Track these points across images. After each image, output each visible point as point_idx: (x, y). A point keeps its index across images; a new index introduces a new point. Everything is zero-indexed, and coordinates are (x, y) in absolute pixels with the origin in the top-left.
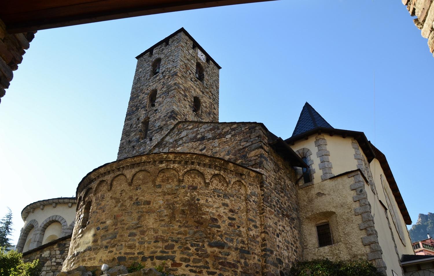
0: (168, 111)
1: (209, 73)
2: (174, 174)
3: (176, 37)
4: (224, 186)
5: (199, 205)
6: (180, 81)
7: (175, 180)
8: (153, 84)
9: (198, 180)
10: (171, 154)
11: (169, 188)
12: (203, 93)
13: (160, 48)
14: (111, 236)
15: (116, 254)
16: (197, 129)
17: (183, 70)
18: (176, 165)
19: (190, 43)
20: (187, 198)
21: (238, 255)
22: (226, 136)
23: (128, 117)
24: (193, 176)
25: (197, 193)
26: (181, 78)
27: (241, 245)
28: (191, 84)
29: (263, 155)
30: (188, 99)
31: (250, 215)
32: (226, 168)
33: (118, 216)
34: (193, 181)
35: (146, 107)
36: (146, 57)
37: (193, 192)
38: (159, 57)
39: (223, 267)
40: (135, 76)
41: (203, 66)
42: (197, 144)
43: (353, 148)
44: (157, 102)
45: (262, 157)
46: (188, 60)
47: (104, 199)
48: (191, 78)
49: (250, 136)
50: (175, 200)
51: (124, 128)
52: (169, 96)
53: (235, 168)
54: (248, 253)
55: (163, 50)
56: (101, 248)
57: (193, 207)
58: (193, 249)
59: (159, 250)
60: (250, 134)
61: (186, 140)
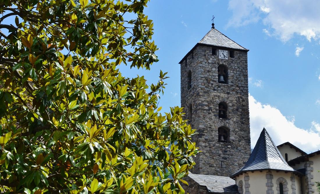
12: (228, 93)
17: (204, 87)
19: (209, 52)
43: (266, 178)
46: (209, 71)
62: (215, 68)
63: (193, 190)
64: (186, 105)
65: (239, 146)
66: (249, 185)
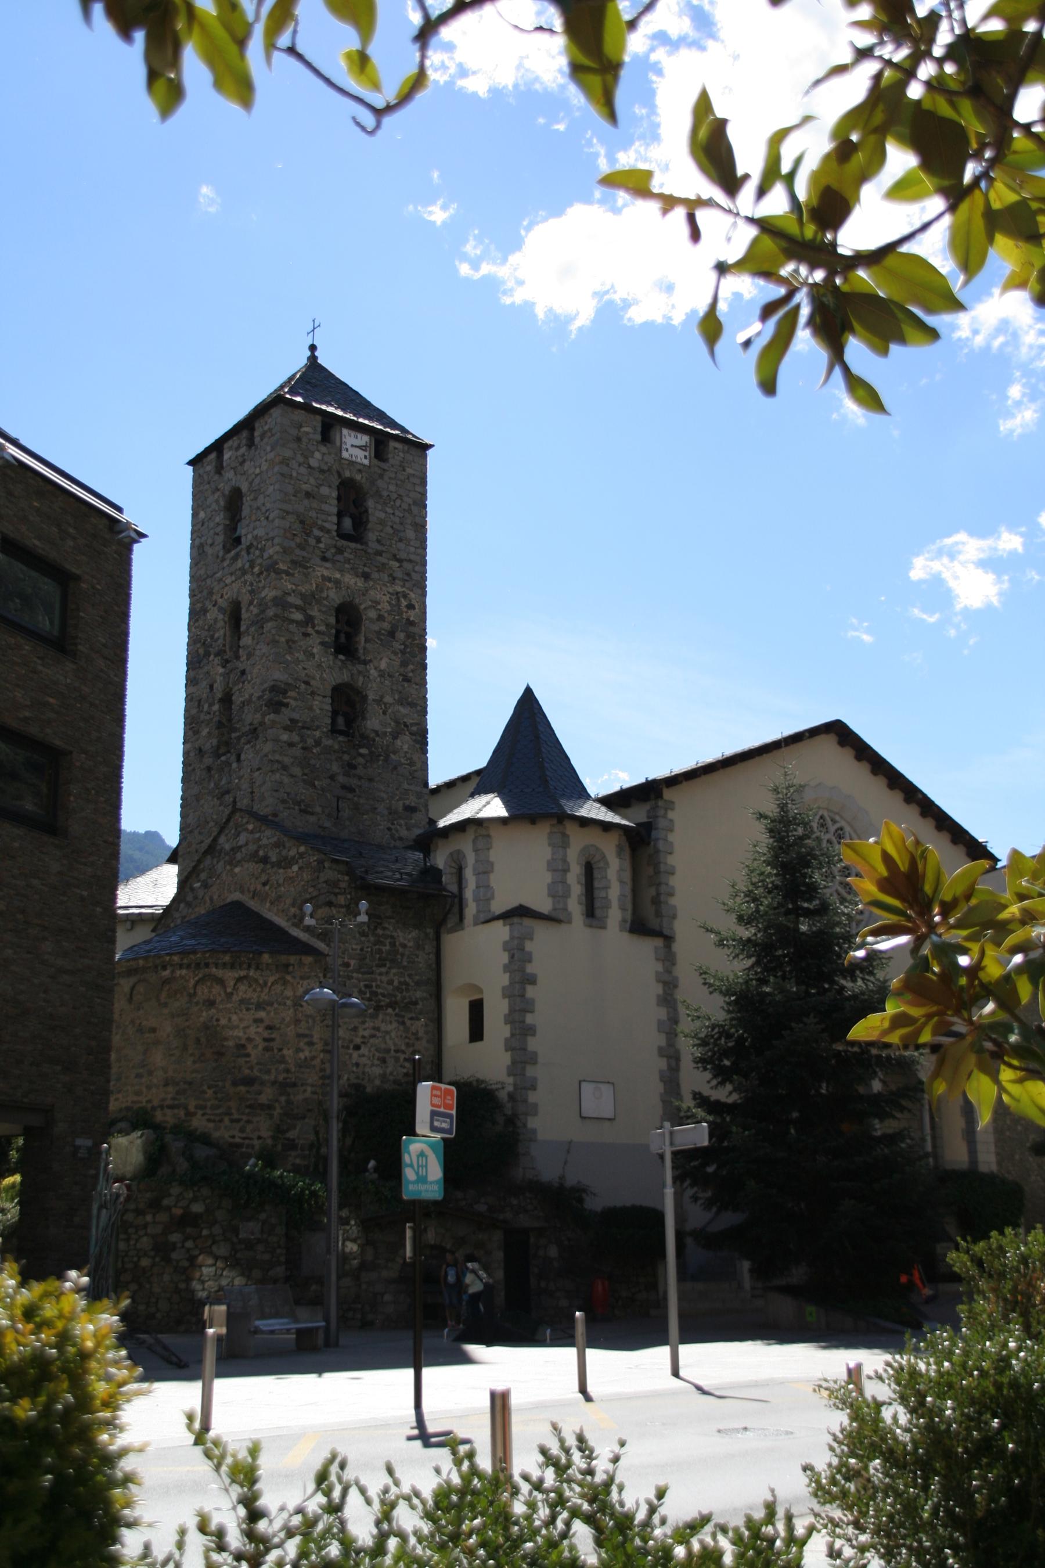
1: (385, 494)
9: (217, 989)
12: (366, 576)
18: (184, 972)
24: (209, 984)
26: (288, 574)
30: (317, 628)
35: (225, 651)
41: (364, 480)
43: (550, 845)
46: (308, 495)
50: (187, 1024)
54: (294, 1085)
58: (210, 1092)
59: (170, 1096)
62: (330, 487)
63: (291, 875)
64: (214, 606)
65: (394, 753)
66: (492, 864)
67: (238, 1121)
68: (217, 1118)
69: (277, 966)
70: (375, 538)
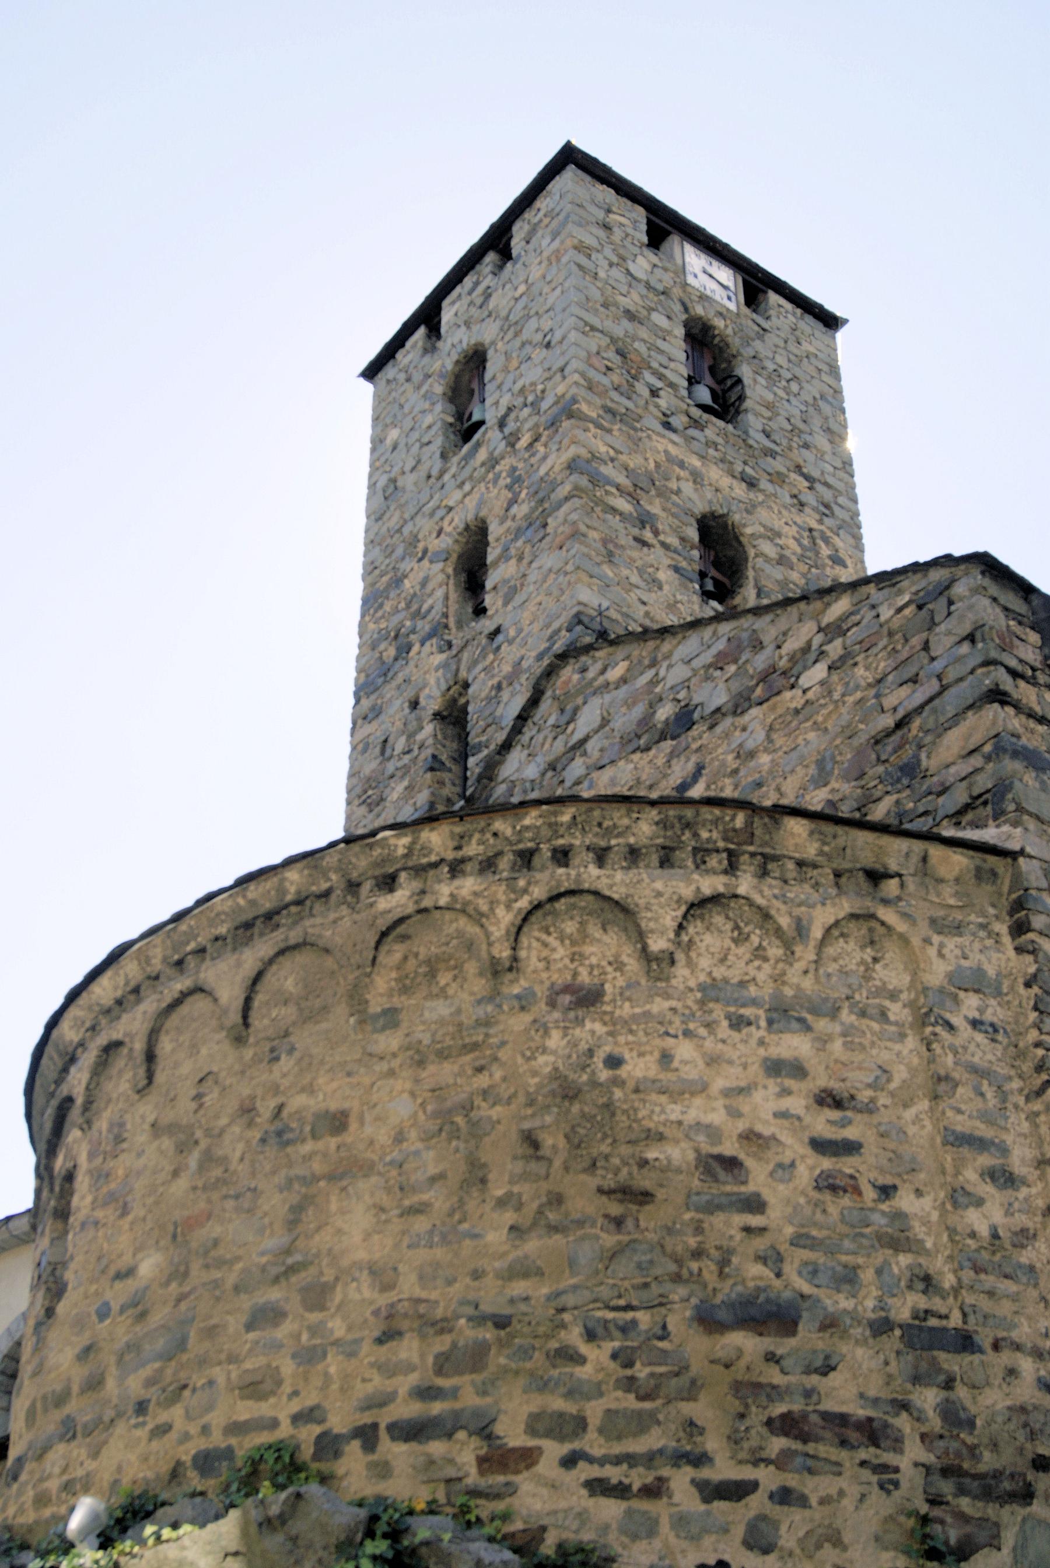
0: (556, 625)
1: (771, 366)
2: (460, 934)
3: (543, 203)
4: (766, 959)
5: (618, 1094)
6: (600, 444)
7: (471, 968)
8: (465, 496)
9: (606, 945)
10: (435, 824)
11: (442, 1022)
12: (751, 484)
13: (470, 293)
14: (160, 1344)
15: (186, 1437)
16: (653, 672)
17: (605, 381)
18: (468, 885)
19: (633, 222)
20: (546, 1064)
21: (893, 1363)
22: (798, 677)
23: (366, 703)
24: (570, 927)
25: (605, 1024)
27: (916, 1300)
28: (671, 449)
29: (1014, 740)
30: (662, 537)
31: (959, 1111)
32: (767, 850)
33: (192, 1223)
34: (572, 960)
35: (446, 626)
36: (410, 357)
37: (579, 1022)
38: (473, 342)
39: (797, 1446)
40: (370, 476)
41: (729, 331)
42: (660, 761)
44: (495, 588)
45: (1005, 751)
46: (630, 316)
47: (125, 1145)
48: (664, 415)
49: (926, 647)
50: (483, 1081)
51: (351, 767)
52: (548, 539)
53: (824, 843)
54: (965, 1343)
55: (487, 295)
56: (120, 1415)
57: (586, 1109)
58: (597, 1358)
59: (405, 1384)
60: (925, 635)
61: (601, 750)
67: (736, 1491)
68: (638, 1477)
69: (838, 875)
70: (760, 428)
